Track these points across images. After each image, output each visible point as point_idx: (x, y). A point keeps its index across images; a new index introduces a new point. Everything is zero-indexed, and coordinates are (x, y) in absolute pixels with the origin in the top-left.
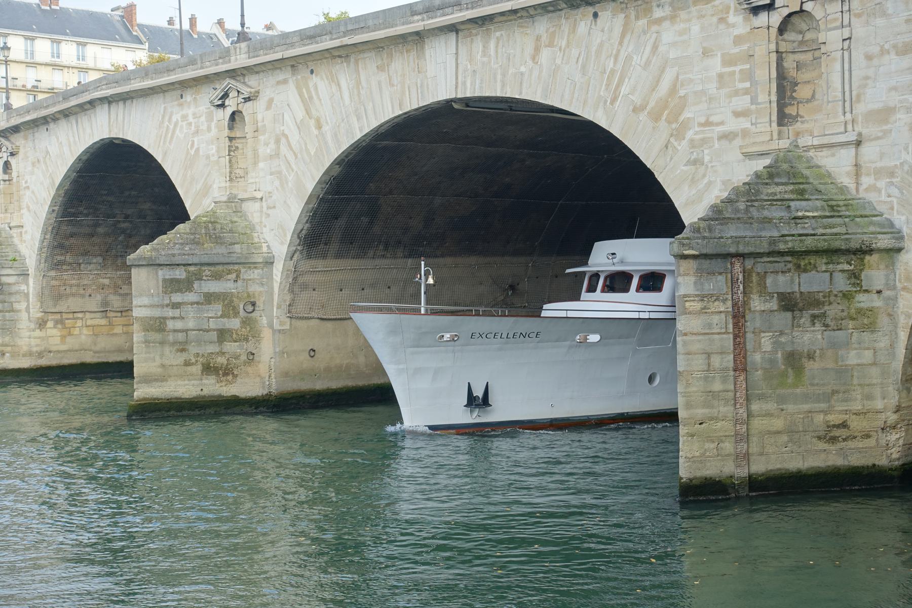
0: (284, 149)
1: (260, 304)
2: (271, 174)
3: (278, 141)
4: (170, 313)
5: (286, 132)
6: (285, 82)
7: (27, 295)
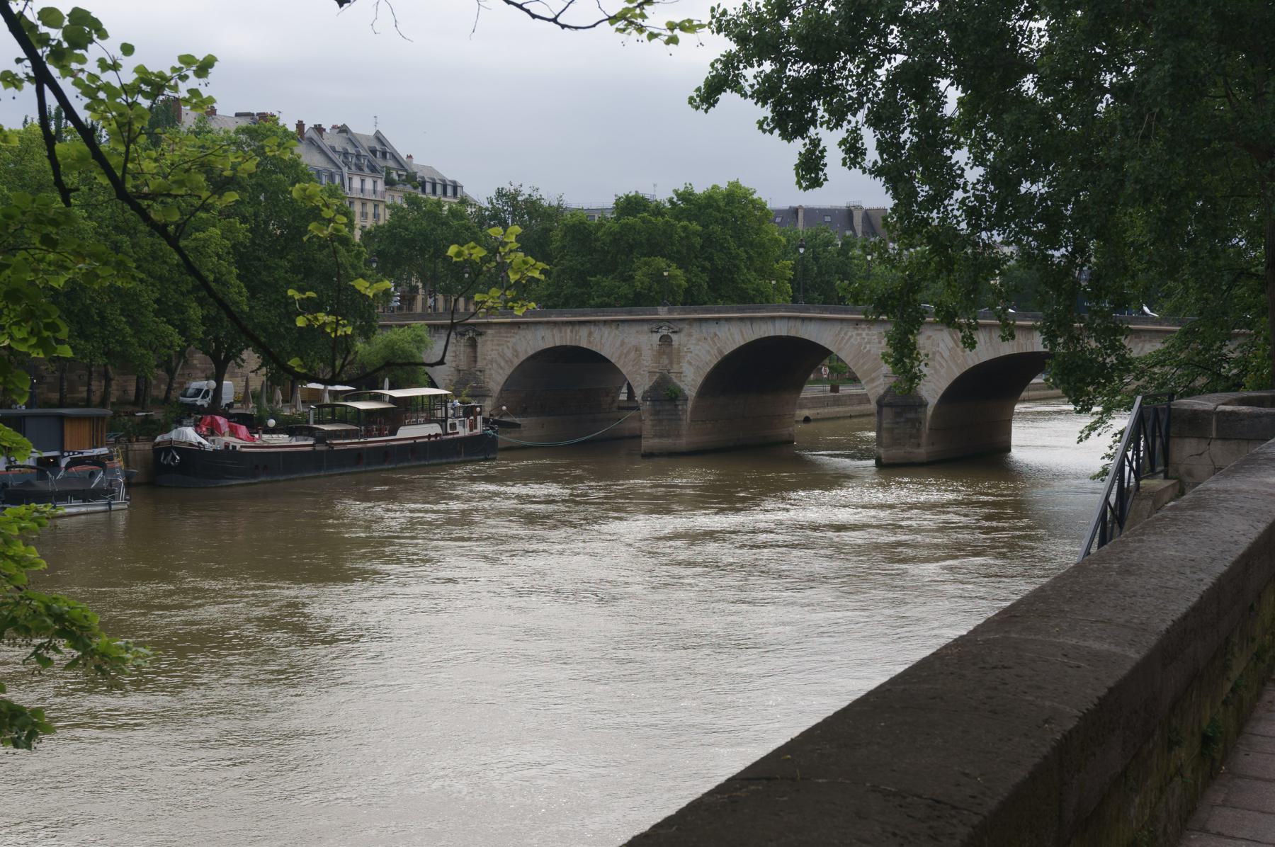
1: (923, 422)
6: (942, 330)
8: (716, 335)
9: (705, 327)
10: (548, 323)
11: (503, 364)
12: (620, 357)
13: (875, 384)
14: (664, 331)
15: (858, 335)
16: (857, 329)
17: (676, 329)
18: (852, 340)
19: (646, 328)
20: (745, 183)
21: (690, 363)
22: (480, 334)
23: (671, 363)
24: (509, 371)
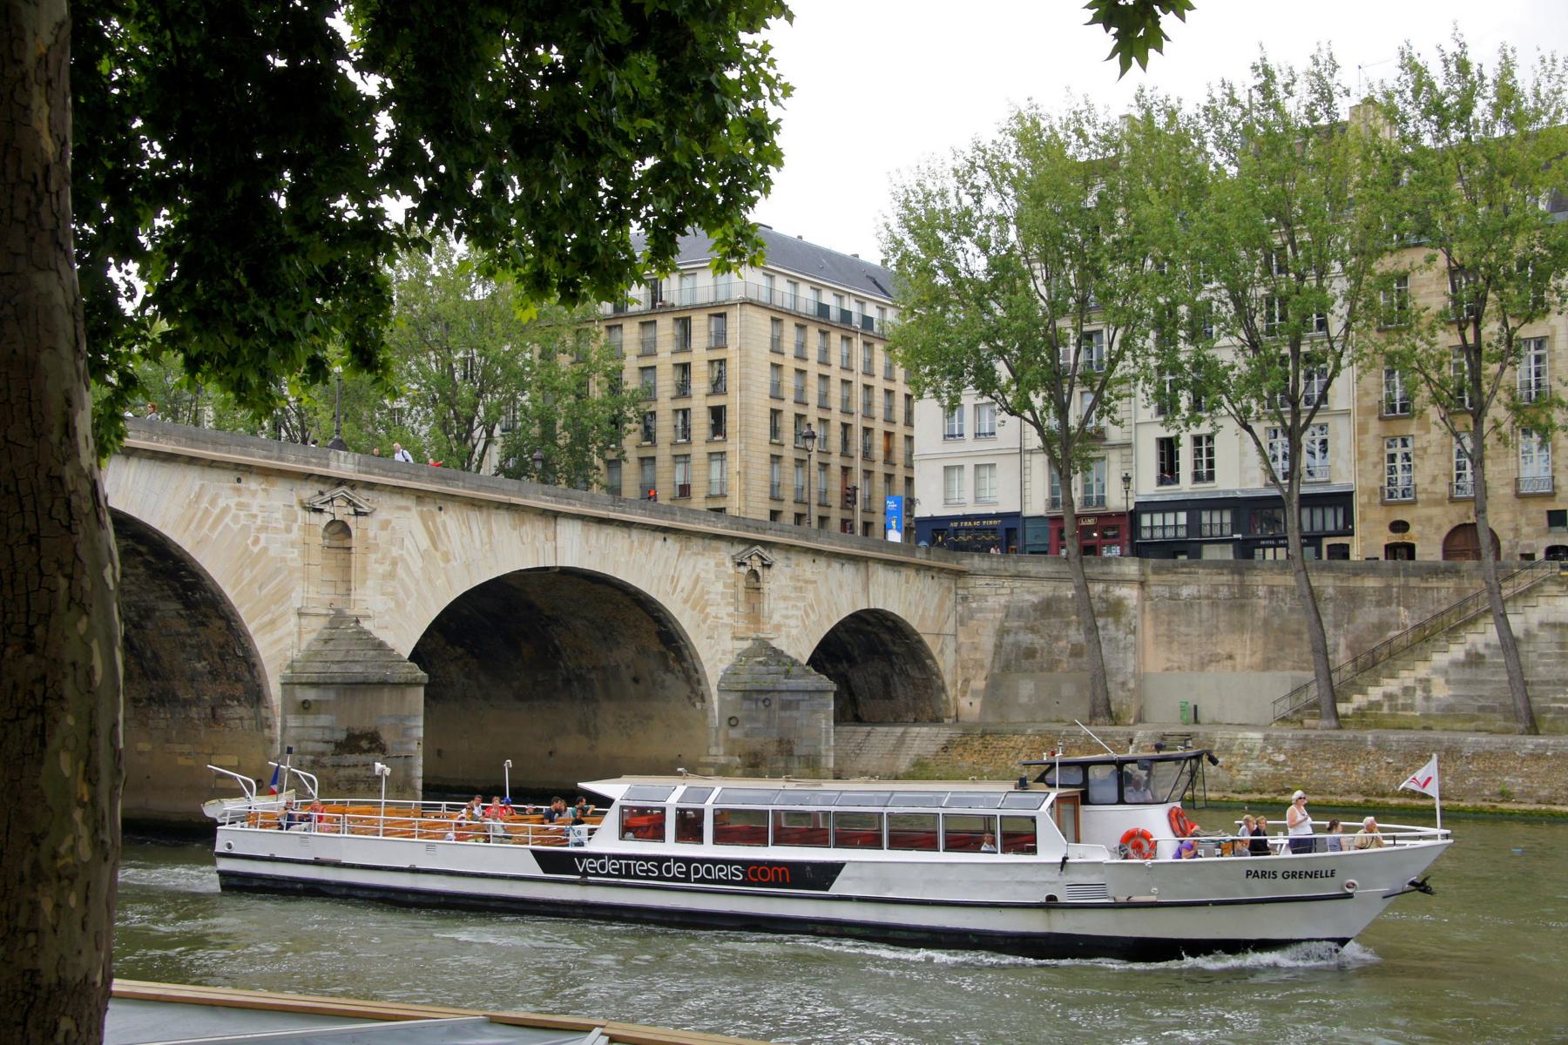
0: (401, 572)
2: (383, 594)
3: (394, 563)
5: (407, 557)
6: (407, 509)
13: (277, 635)
15: (240, 506)
18: (228, 519)
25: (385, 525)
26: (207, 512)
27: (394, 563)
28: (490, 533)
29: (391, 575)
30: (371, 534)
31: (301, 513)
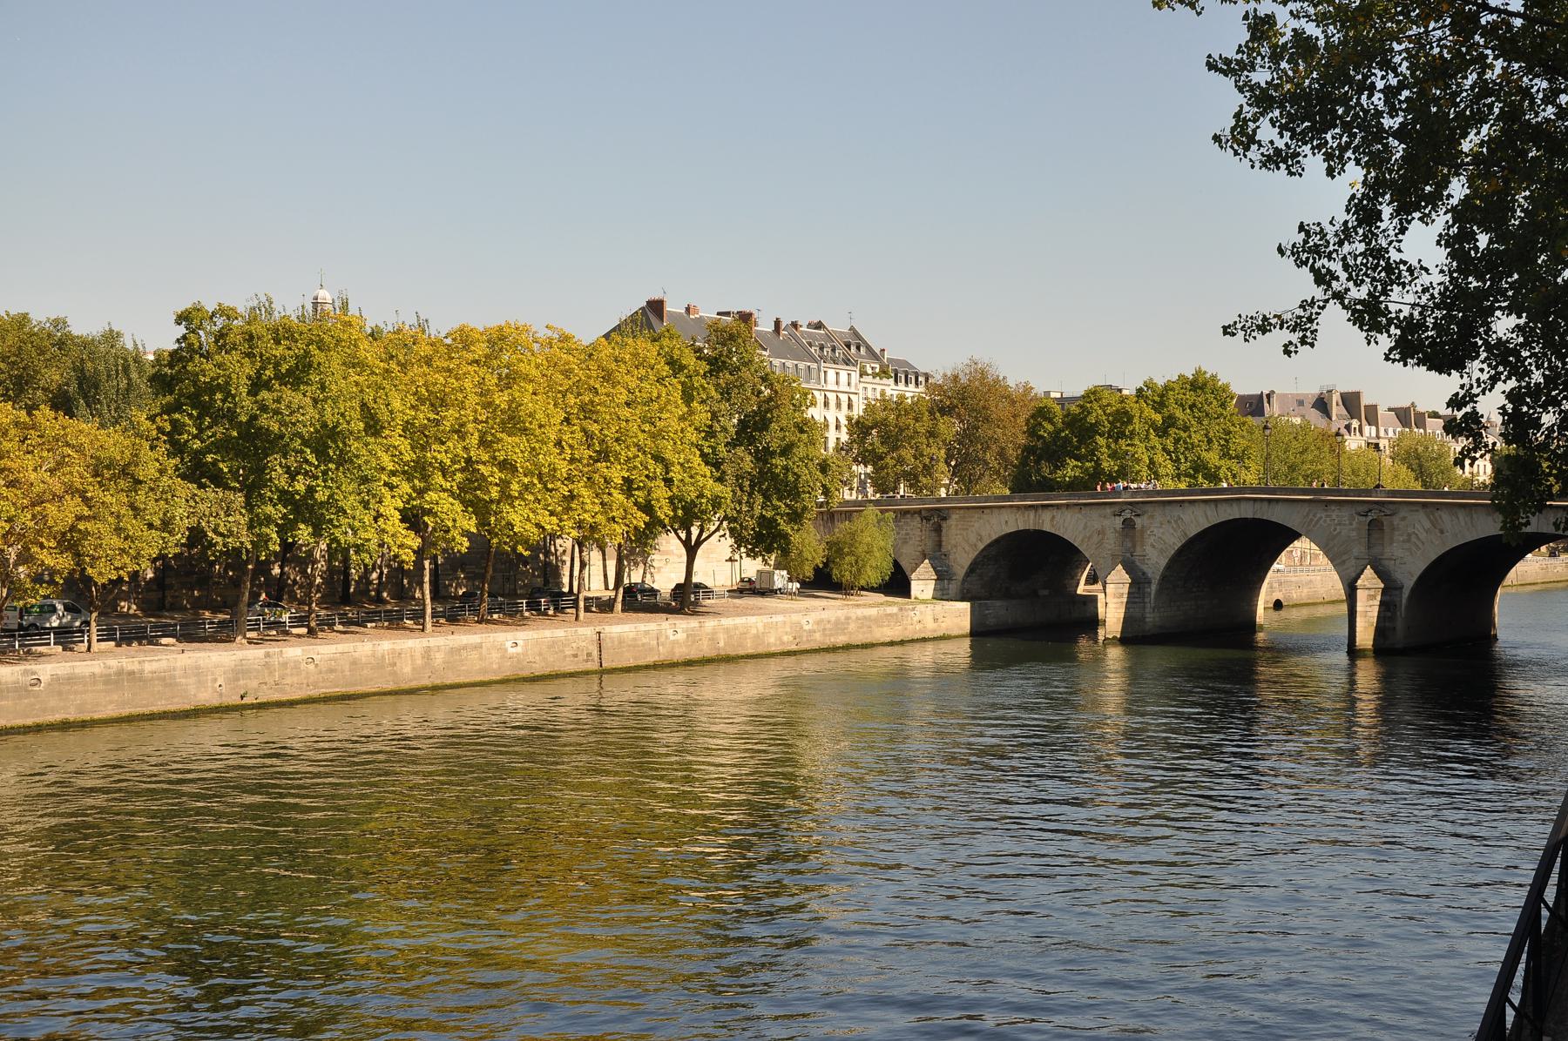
0: (1414, 539)
4: (1369, 609)
6: (1417, 511)
7: (1150, 594)
8: (1180, 518)
9: (1168, 508)
10: (1011, 506)
11: (967, 548)
12: (1082, 541)
14: (1127, 514)
15: (1327, 516)
16: (1326, 510)
17: (1139, 512)
18: (1321, 522)
19: (1108, 511)
20: (1210, 369)
21: (1154, 547)
22: (945, 519)
23: (1134, 546)
24: (973, 555)
25: (1404, 519)
26: (1312, 520)
27: (1409, 535)
28: (1472, 517)
29: (1409, 541)
30: (1395, 523)
31: (1357, 517)
